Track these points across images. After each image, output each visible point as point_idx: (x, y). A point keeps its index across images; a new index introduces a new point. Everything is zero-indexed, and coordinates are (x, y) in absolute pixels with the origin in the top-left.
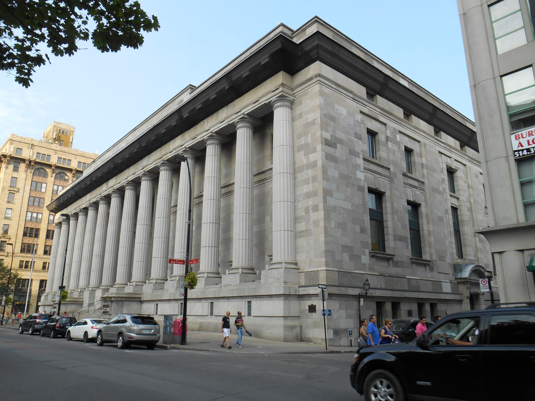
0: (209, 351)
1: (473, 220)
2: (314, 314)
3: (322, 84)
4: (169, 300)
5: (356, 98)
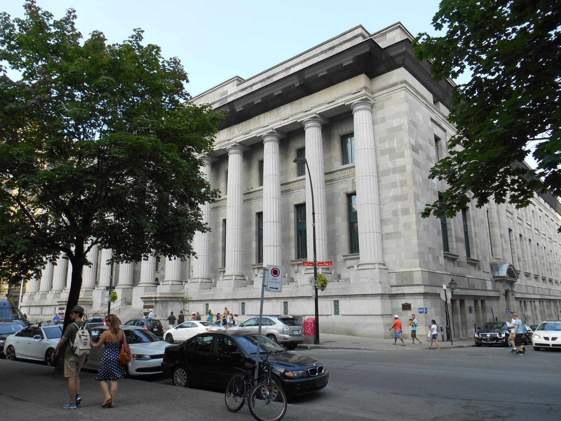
1: (500, 222)
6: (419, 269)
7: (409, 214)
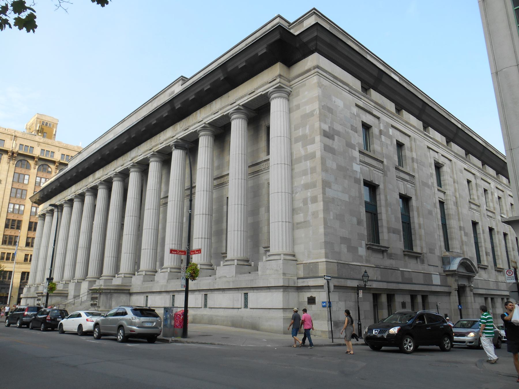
0: (214, 344)
1: (458, 214)
2: (313, 306)
3: (321, 75)
4: (160, 292)
5: (351, 91)
6: (324, 260)
7: (317, 202)
